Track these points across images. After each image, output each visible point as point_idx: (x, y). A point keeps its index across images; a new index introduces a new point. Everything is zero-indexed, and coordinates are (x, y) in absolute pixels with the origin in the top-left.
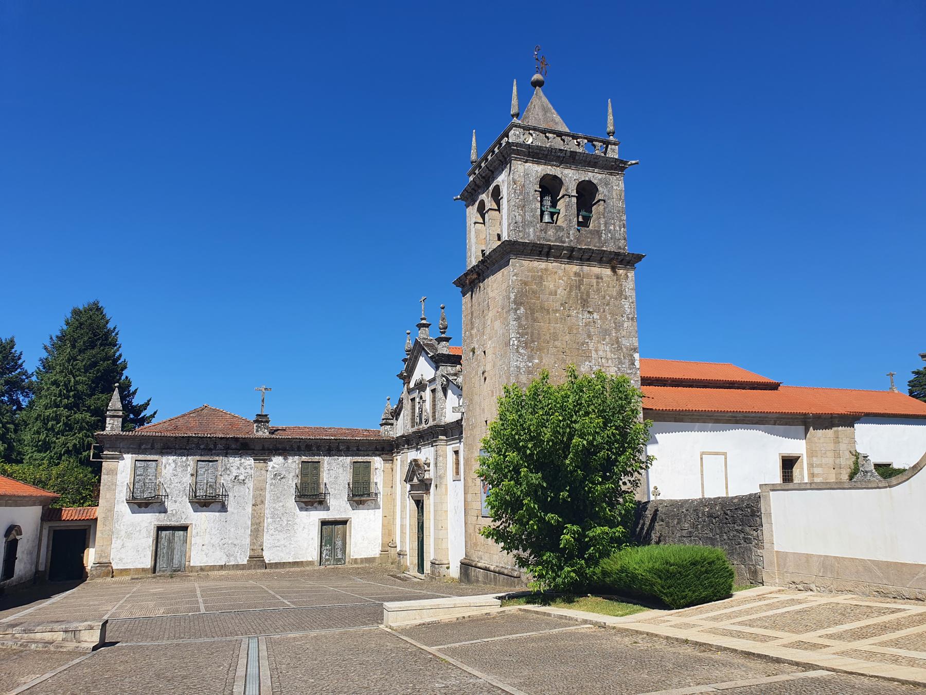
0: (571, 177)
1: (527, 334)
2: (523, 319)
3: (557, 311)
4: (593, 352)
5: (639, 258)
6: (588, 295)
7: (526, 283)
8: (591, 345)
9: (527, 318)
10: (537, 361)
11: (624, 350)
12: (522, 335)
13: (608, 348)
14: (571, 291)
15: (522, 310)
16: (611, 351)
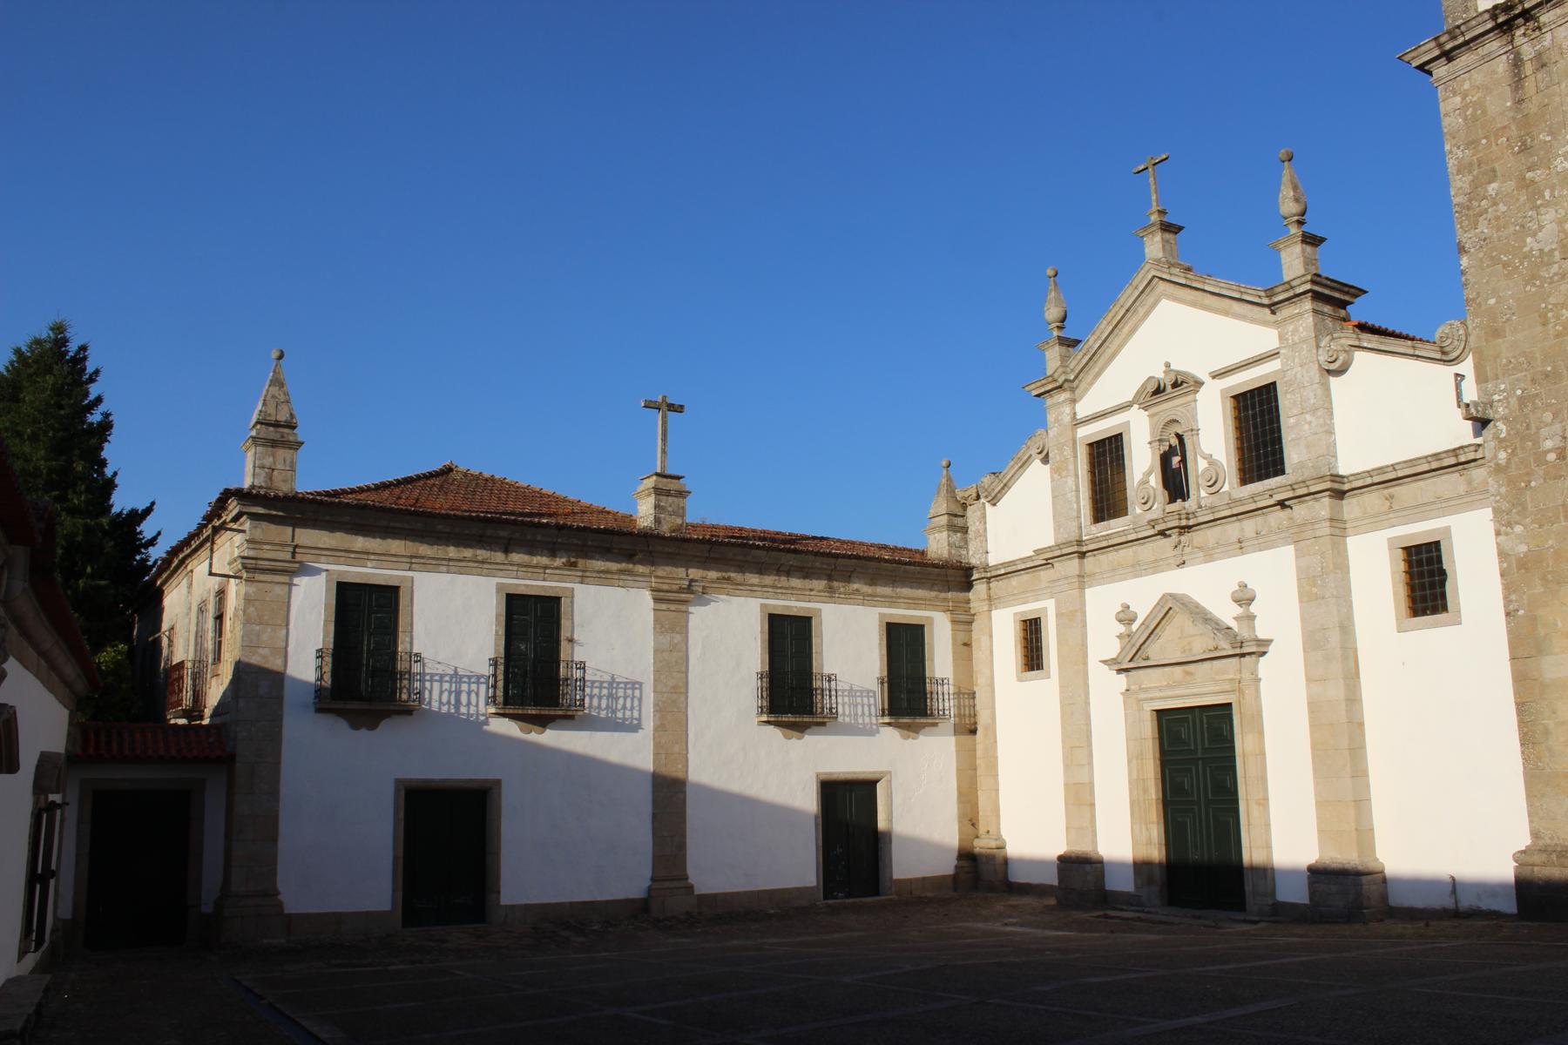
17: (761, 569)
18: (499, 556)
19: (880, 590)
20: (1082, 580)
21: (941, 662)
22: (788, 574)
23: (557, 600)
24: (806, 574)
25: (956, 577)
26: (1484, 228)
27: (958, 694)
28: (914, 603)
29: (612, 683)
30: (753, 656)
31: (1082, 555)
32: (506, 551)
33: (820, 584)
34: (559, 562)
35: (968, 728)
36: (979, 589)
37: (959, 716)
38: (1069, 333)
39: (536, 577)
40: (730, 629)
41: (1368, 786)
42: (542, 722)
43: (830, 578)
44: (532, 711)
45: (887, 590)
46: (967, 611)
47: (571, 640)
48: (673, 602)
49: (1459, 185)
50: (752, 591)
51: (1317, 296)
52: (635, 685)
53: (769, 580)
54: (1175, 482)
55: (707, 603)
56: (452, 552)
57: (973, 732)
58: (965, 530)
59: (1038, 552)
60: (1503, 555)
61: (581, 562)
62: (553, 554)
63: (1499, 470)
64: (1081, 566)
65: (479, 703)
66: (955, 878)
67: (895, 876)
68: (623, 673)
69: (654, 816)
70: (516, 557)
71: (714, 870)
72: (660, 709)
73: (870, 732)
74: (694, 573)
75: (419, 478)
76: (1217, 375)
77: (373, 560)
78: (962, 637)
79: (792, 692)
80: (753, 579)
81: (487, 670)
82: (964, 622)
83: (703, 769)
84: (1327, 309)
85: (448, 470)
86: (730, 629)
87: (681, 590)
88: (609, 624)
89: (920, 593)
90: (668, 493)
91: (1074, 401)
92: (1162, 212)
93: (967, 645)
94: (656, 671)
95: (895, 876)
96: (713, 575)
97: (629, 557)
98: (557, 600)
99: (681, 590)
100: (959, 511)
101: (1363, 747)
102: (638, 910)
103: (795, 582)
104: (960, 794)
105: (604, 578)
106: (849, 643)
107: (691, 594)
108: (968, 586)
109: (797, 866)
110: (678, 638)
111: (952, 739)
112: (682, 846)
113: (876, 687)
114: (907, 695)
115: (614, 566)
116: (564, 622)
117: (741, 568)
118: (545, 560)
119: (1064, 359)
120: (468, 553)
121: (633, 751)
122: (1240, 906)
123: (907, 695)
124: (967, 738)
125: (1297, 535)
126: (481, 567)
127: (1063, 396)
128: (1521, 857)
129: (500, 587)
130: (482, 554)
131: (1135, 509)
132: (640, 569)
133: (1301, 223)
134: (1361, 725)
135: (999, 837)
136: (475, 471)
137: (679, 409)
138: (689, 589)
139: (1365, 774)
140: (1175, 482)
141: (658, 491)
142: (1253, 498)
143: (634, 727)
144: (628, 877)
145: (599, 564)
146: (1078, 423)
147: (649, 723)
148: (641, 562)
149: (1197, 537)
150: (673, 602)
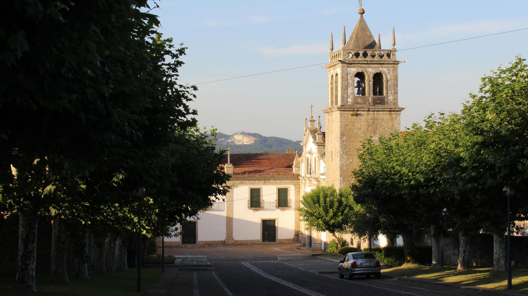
1: (347, 148)
5: (403, 109)
6: (377, 128)
7: (347, 125)
9: (347, 141)
12: (344, 149)
19: (277, 182)
22: (255, 180)
28: (285, 184)
45: (279, 182)
46: (299, 185)
53: (251, 182)
58: (299, 167)
67: (279, 238)
71: (238, 236)
72: (228, 207)
73: (275, 210)
74: (234, 182)
79: (255, 201)
80: (247, 182)
89: (287, 181)
96: (239, 182)
102: (223, 243)
103: (257, 182)
109: (257, 235)
111: (294, 211)
112: (232, 232)
117: (245, 180)
143: (223, 211)
144: (222, 237)
147: (226, 210)
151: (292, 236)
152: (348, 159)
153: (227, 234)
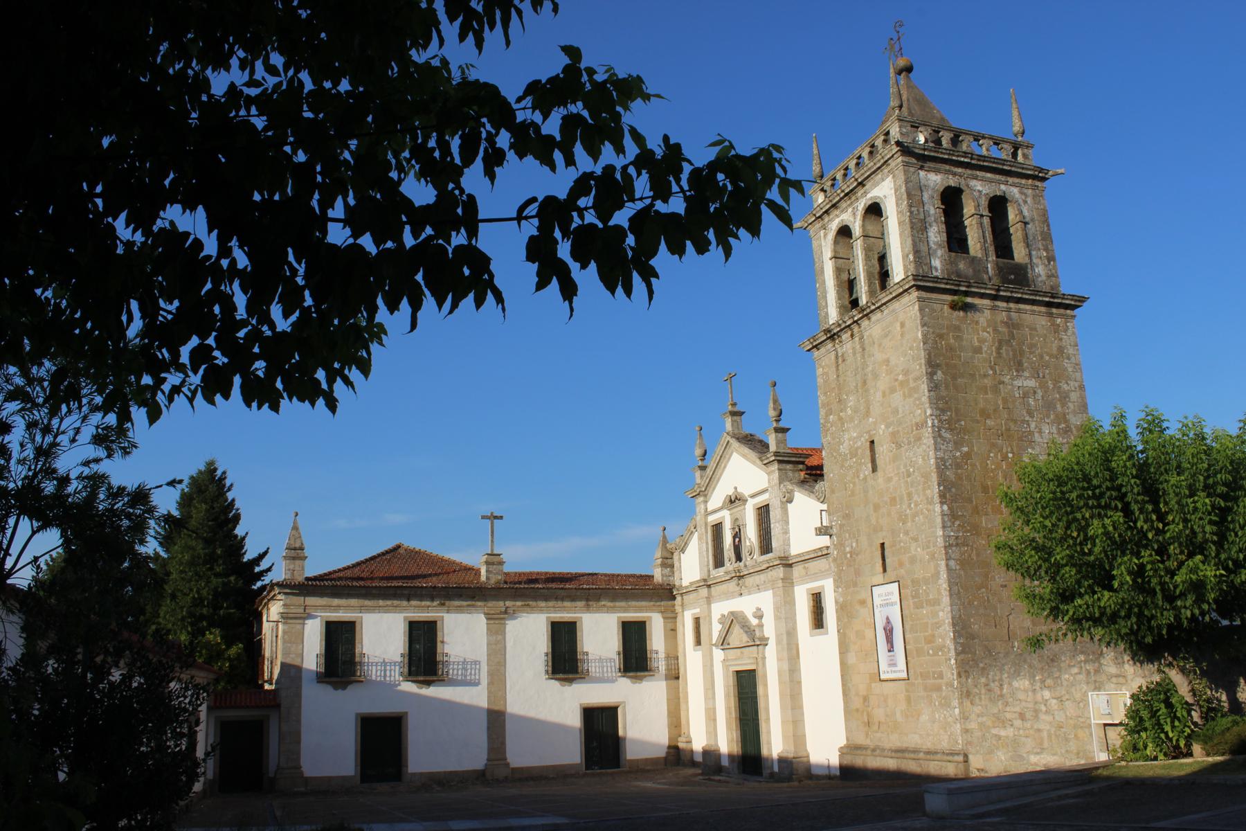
0: (979, 189)
1: (950, 409)
2: (943, 388)
3: (985, 376)
4: (1036, 435)
5: (1082, 300)
6: (1022, 353)
7: (941, 336)
8: (1033, 425)
9: (947, 387)
10: (966, 449)
11: (1075, 432)
12: (943, 411)
13: (1054, 430)
14: (999, 349)
15: (939, 375)
16: (1058, 433)
17: (546, 599)
18: (405, 603)
19: (617, 604)
20: (709, 600)
21: (657, 641)
22: (563, 600)
23: (435, 622)
24: (573, 599)
25: (666, 594)
26: (829, 438)
27: (668, 657)
28: (640, 610)
29: (465, 662)
30: (542, 644)
31: (709, 586)
32: (408, 600)
33: (581, 604)
34: (435, 603)
35: (674, 676)
36: (679, 598)
37: (668, 669)
38: (781, 425)
39: (423, 612)
40: (530, 631)
41: (803, 714)
42: (428, 683)
43: (587, 600)
44: (421, 678)
45: (623, 604)
46: (673, 611)
47: (443, 642)
48: (497, 621)
49: (822, 412)
50: (541, 611)
51: (780, 462)
52: (476, 662)
53: (551, 604)
54: (737, 550)
55: (515, 618)
56: (381, 602)
57: (678, 678)
58: (672, 566)
59: (691, 584)
60: (836, 602)
61: (447, 603)
62: (432, 599)
63: (835, 560)
64: (709, 593)
65: (395, 675)
66: (666, 759)
67: (628, 757)
68: (470, 657)
69: (488, 728)
70: (413, 603)
71: (519, 756)
72: (491, 674)
73: (613, 681)
74: (508, 603)
75: (379, 555)
76: (753, 496)
77: (342, 610)
78: (670, 626)
79: (565, 659)
80: (543, 604)
81: (399, 659)
82: (672, 619)
83: (515, 705)
84: (789, 467)
85: (399, 547)
86: (530, 631)
87: (501, 613)
88: (463, 633)
89: (644, 603)
90: (493, 564)
91: (706, 502)
92: (734, 405)
93: (674, 630)
94: (488, 655)
95: (628, 757)
96: (519, 603)
97: (473, 598)
98: (435, 622)
99: (501, 613)
100: (668, 555)
101: (800, 693)
102: (480, 776)
103: (567, 604)
104: (669, 712)
105: (459, 610)
106: (600, 634)
107: (507, 614)
108: (674, 598)
109: (572, 753)
110: (500, 637)
111: (664, 683)
112: (503, 743)
113: (616, 657)
114: (635, 658)
115: (465, 603)
116: (439, 634)
117: (535, 598)
118: (428, 603)
119: (702, 477)
120: (389, 602)
121: (477, 697)
122: (760, 774)
123: (635, 658)
124: (673, 682)
125: (771, 585)
126: (395, 609)
127: (701, 499)
128: (843, 752)
129: (405, 618)
130: (396, 602)
131: (727, 564)
132: (479, 603)
133: (777, 421)
134: (800, 683)
135: (689, 736)
136: (412, 547)
137: (501, 518)
138: (506, 612)
139: (801, 707)
140: (737, 550)
141: (487, 563)
142: (767, 561)
143: (476, 683)
144: (474, 758)
145: (457, 603)
146: (707, 514)
147: (484, 681)
148: (479, 600)
149: (749, 581)
150: (497, 621)
151: (662, 753)
152: (958, 445)
153: (491, 750)
